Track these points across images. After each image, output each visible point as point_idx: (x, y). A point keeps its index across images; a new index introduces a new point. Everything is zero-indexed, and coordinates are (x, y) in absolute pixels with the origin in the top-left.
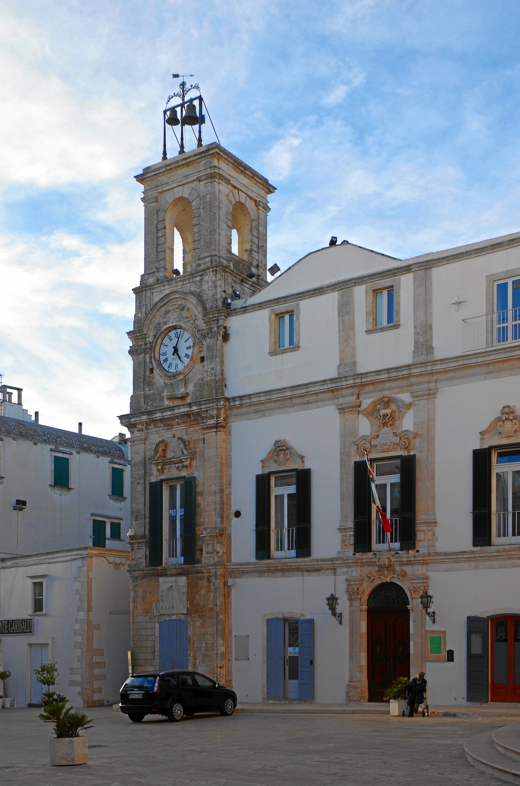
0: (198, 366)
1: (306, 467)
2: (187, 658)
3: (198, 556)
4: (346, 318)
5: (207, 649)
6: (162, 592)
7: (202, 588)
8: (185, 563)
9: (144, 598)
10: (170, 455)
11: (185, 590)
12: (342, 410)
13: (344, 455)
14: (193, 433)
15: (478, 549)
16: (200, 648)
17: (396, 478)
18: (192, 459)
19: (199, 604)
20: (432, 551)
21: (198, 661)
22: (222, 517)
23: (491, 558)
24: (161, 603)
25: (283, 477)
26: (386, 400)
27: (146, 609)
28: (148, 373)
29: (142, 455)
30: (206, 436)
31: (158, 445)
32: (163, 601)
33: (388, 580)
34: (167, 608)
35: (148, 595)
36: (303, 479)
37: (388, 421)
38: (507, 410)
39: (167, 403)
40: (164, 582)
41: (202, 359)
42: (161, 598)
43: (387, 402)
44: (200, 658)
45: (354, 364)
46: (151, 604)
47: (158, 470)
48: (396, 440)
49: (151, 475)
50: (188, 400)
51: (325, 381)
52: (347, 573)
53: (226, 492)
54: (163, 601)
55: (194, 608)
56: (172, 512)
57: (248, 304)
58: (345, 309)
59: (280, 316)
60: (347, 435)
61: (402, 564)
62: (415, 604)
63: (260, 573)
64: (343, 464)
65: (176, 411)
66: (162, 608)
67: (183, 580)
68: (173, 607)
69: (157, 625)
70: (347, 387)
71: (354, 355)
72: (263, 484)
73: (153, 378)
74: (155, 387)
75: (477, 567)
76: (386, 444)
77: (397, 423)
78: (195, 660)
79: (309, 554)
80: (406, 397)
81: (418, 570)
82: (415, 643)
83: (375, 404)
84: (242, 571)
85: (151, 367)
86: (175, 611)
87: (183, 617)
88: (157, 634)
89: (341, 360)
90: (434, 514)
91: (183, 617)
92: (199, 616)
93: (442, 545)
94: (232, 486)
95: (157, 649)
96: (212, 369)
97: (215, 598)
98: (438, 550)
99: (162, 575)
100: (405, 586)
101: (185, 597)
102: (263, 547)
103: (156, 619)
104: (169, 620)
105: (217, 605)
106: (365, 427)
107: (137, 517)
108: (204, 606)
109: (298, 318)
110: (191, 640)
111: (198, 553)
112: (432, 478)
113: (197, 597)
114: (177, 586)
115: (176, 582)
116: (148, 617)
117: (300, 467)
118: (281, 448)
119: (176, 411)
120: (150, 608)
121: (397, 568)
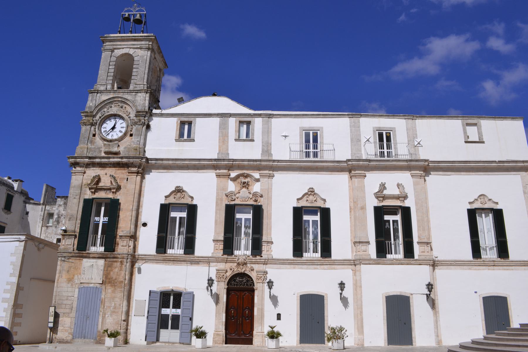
5: (115, 308)
6: (84, 268)
7: (116, 268)
8: (105, 251)
10: (101, 184)
11: (102, 268)
12: (218, 176)
13: (218, 201)
14: (121, 174)
16: (110, 307)
19: (112, 278)
21: (107, 316)
24: (83, 276)
25: (179, 207)
26: (245, 175)
28: (91, 136)
29: (81, 182)
30: (129, 177)
31: (94, 177)
32: (84, 274)
33: (243, 271)
34: (87, 279)
35: (72, 269)
36: (192, 210)
37: (245, 185)
38: (311, 190)
39: (103, 155)
42: (82, 272)
43: (247, 176)
44: (109, 313)
45: (228, 154)
46: (74, 275)
47: (92, 192)
49: (85, 194)
54: (84, 274)
57: (162, 112)
58: (223, 128)
60: (220, 189)
66: (83, 278)
67: (101, 262)
68: (92, 279)
69: (77, 290)
70: (221, 165)
72: (165, 209)
73: (95, 139)
74: (95, 144)
77: (250, 188)
82: (258, 309)
84: (147, 259)
85: (94, 133)
87: (98, 286)
88: (76, 295)
89: (219, 151)
92: (112, 286)
95: (75, 305)
99: (86, 257)
101: (102, 273)
103: (77, 286)
104: (87, 287)
107: (70, 218)
108: (116, 279)
109: (195, 125)
113: (112, 273)
115: (96, 262)
116: (70, 284)
117: (190, 203)
118: (179, 190)
120: (73, 278)
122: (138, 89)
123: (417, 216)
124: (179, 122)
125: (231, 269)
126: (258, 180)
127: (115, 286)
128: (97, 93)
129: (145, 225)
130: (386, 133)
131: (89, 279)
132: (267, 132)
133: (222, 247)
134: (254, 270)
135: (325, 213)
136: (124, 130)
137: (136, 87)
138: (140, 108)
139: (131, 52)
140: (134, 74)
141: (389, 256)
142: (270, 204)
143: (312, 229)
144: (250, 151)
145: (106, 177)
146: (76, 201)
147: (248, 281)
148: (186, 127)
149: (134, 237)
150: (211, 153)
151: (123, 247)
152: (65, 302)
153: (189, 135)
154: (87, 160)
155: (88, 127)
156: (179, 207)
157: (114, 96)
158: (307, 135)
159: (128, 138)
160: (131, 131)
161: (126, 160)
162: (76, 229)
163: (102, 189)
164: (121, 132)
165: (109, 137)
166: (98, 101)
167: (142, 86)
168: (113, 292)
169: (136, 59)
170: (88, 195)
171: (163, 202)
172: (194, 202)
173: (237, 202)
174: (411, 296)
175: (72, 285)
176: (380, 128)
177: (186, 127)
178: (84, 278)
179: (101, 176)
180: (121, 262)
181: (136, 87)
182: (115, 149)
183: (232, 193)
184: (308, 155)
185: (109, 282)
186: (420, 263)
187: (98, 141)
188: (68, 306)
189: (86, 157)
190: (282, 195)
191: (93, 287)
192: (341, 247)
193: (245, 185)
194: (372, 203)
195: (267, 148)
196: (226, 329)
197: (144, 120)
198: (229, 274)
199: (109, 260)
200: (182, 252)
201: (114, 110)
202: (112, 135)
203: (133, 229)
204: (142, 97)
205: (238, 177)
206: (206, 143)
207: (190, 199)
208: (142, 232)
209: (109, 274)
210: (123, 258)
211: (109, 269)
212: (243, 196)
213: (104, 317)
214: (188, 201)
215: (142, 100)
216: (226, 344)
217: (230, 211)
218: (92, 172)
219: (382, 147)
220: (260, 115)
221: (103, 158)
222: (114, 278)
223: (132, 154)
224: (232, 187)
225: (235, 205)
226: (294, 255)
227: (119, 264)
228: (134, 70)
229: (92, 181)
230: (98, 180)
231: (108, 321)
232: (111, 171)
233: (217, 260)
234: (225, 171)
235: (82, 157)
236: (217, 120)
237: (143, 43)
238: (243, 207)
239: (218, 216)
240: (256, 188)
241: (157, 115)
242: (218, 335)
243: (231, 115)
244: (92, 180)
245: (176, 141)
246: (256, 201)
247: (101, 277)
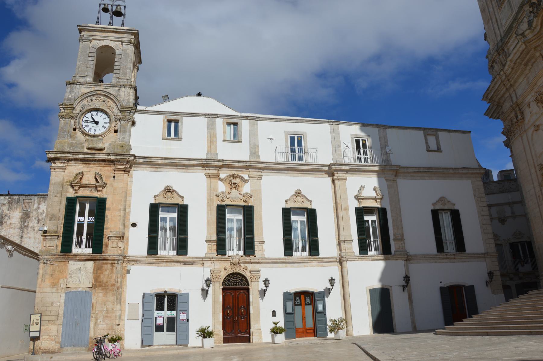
0: (113, 134)
1: (185, 203)
2: (89, 318)
3: (103, 249)
4: (212, 131)
5: (107, 312)
6: (71, 271)
7: (106, 270)
8: (93, 253)
9: (52, 275)
11: (92, 271)
12: (209, 176)
14: (106, 171)
15: (286, 257)
16: (101, 311)
18: (104, 187)
19: (103, 281)
20: (263, 257)
21: (99, 321)
22: (124, 225)
23: (294, 262)
24: (69, 280)
25: (169, 207)
27: (53, 283)
28: (72, 130)
29: (61, 179)
30: (116, 175)
31: (77, 175)
32: (71, 277)
34: (74, 282)
35: (56, 273)
38: (299, 192)
39: (86, 150)
40: (73, 265)
41: (116, 131)
44: (101, 318)
45: (217, 154)
46: (59, 279)
48: (241, 197)
49: (67, 192)
50: (104, 152)
51: (201, 159)
52: (211, 266)
53: (127, 211)
54: (71, 277)
56: (81, 219)
57: (147, 109)
58: (211, 128)
59: (169, 121)
60: (211, 190)
61: (246, 262)
63: (150, 263)
64: (209, 205)
65: (96, 156)
66: (70, 282)
68: (80, 282)
69: (63, 295)
71: (216, 150)
72: (154, 209)
73: (76, 134)
74: (76, 139)
75: (286, 266)
76: (235, 197)
77: (240, 189)
78: (97, 319)
79: (186, 254)
80: (246, 177)
81: (256, 267)
83: (229, 177)
85: (74, 127)
86: (82, 285)
87: (88, 289)
88: (63, 300)
89: (208, 151)
90: (263, 237)
92: (102, 289)
93: (268, 254)
94: (131, 208)
95: (61, 312)
96: (124, 138)
97: (117, 277)
98: (266, 257)
99: (72, 259)
100: (247, 274)
101: (91, 276)
102: (153, 247)
103: (63, 290)
104: (75, 292)
106: (222, 187)
108: (107, 282)
109: (182, 124)
110: (95, 306)
111: (104, 247)
112: (261, 219)
113: (102, 276)
114: (85, 268)
115: (84, 265)
116: (55, 289)
117: (180, 203)
118: (168, 190)
119: (96, 156)
120: (58, 282)
121: (242, 265)
122: (122, 83)
123: (392, 216)
124: (166, 120)
125: (225, 269)
126: (247, 181)
127: (106, 289)
128: (77, 84)
129: (134, 225)
130: (362, 140)
131: (76, 283)
132: (254, 134)
133: (215, 247)
134: (247, 268)
135: (311, 214)
136: (107, 125)
137: (119, 82)
138: (124, 104)
139: (112, 44)
140: (115, 67)
141: (369, 253)
142: (260, 204)
144: (238, 153)
145: (89, 173)
146: (57, 199)
147: (242, 280)
148: (173, 124)
150: (200, 153)
151: (111, 248)
152: (50, 309)
153: (176, 134)
154: (69, 155)
155: (68, 120)
156: (169, 207)
157: (96, 89)
158: (292, 139)
161: (113, 157)
162: (59, 229)
163: (86, 187)
164: (104, 127)
165: (92, 133)
166: (77, 93)
168: (105, 296)
169: (117, 52)
170: (71, 193)
171: (153, 202)
172: (185, 203)
173: (228, 202)
174: (390, 288)
175: (57, 290)
177: (173, 126)
178: (71, 282)
179: (85, 173)
180: (112, 265)
181: (119, 82)
182: (100, 146)
183: (223, 193)
184: (293, 158)
187: (82, 138)
188: (53, 313)
189: (69, 153)
190: (271, 197)
191: (82, 292)
193: (235, 186)
194: (354, 204)
195: (254, 150)
196: (224, 328)
198: (223, 275)
199: (98, 262)
200: (174, 252)
201: (98, 104)
202: (95, 130)
204: (126, 93)
206: (193, 142)
207: (181, 199)
208: (132, 233)
209: (99, 276)
210: (114, 260)
211: (99, 271)
213: (96, 323)
214: (179, 201)
216: (224, 343)
217: (221, 211)
218: (74, 169)
219: (359, 153)
220: (247, 118)
221: (88, 154)
222: (105, 281)
223: (119, 151)
225: (227, 206)
226: (285, 255)
227: (109, 266)
228: (116, 64)
230: (81, 175)
231: (100, 326)
232: (95, 168)
233: (212, 261)
234: (215, 172)
235: (64, 153)
236: (205, 120)
237: (125, 36)
238: (235, 208)
240: (246, 189)
241: (141, 112)
244: (75, 177)
245: (163, 139)
246: (245, 201)
247: (91, 280)
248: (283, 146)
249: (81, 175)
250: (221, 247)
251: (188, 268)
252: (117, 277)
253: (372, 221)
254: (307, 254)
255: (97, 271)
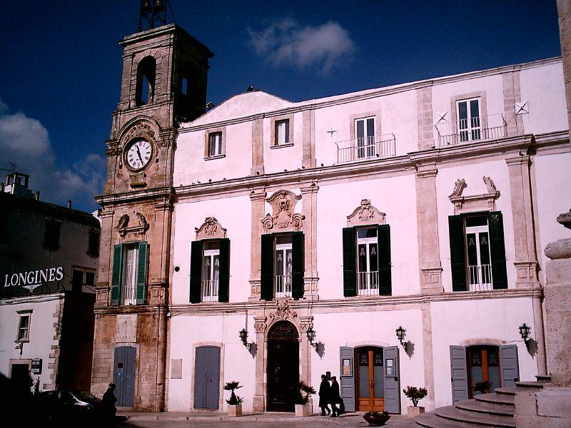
5: (149, 370)
10: (130, 225)
11: (135, 324)
13: (255, 228)
17: (289, 246)
24: (118, 334)
26: (283, 192)
31: (122, 218)
37: (285, 206)
40: (121, 318)
41: (157, 161)
46: (110, 335)
47: (121, 236)
49: (115, 239)
55: (142, 338)
60: (256, 214)
62: (303, 337)
67: (134, 317)
70: (256, 184)
72: (197, 248)
76: (284, 225)
81: (304, 313)
82: (303, 366)
84: (179, 311)
91: (133, 345)
101: (135, 330)
102: (196, 295)
105: (158, 336)
118: (210, 222)
123: (515, 223)
126: (299, 197)
129: (177, 269)
132: (310, 127)
134: (299, 317)
141: (473, 288)
142: (314, 228)
143: (368, 258)
146: (107, 248)
148: (217, 138)
149: (166, 285)
151: (156, 299)
152: (103, 365)
159: (153, 165)
160: (157, 155)
161: (152, 193)
167: (165, 96)
168: (147, 351)
170: (118, 240)
173: (276, 230)
176: (460, 96)
182: (141, 181)
184: (361, 154)
185: (144, 341)
186: (517, 293)
190: (327, 217)
191: (128, 347)
192: (405, 275)
194: (449, 210)
196: (268, 392)
197: (169, 140)
203: (163, 276)
205: (276, 195)
211: (143, 324)
212: (282, 221)
215: (165, 113)
217: (268, 243)
218: (121, 211)
220: (300, 109)
224: (269, 209)
226: (346, 295)
227: (151, 317)
228: (157, 77)
229: (120, 222)
232: (139, 208)
236: (250, 124)
239: (254, 250)
241: (186, 130)
242: (257, 399)
243: (264, 116)
244: (119, 221)
245: (206, 159)
248: (346, 138)
249: (126, 219)
250: (267, 291)
251: (231, 317)
252: (158, 330)
253: (481, 235)
254: (490, 287)
255: (141, 323)
